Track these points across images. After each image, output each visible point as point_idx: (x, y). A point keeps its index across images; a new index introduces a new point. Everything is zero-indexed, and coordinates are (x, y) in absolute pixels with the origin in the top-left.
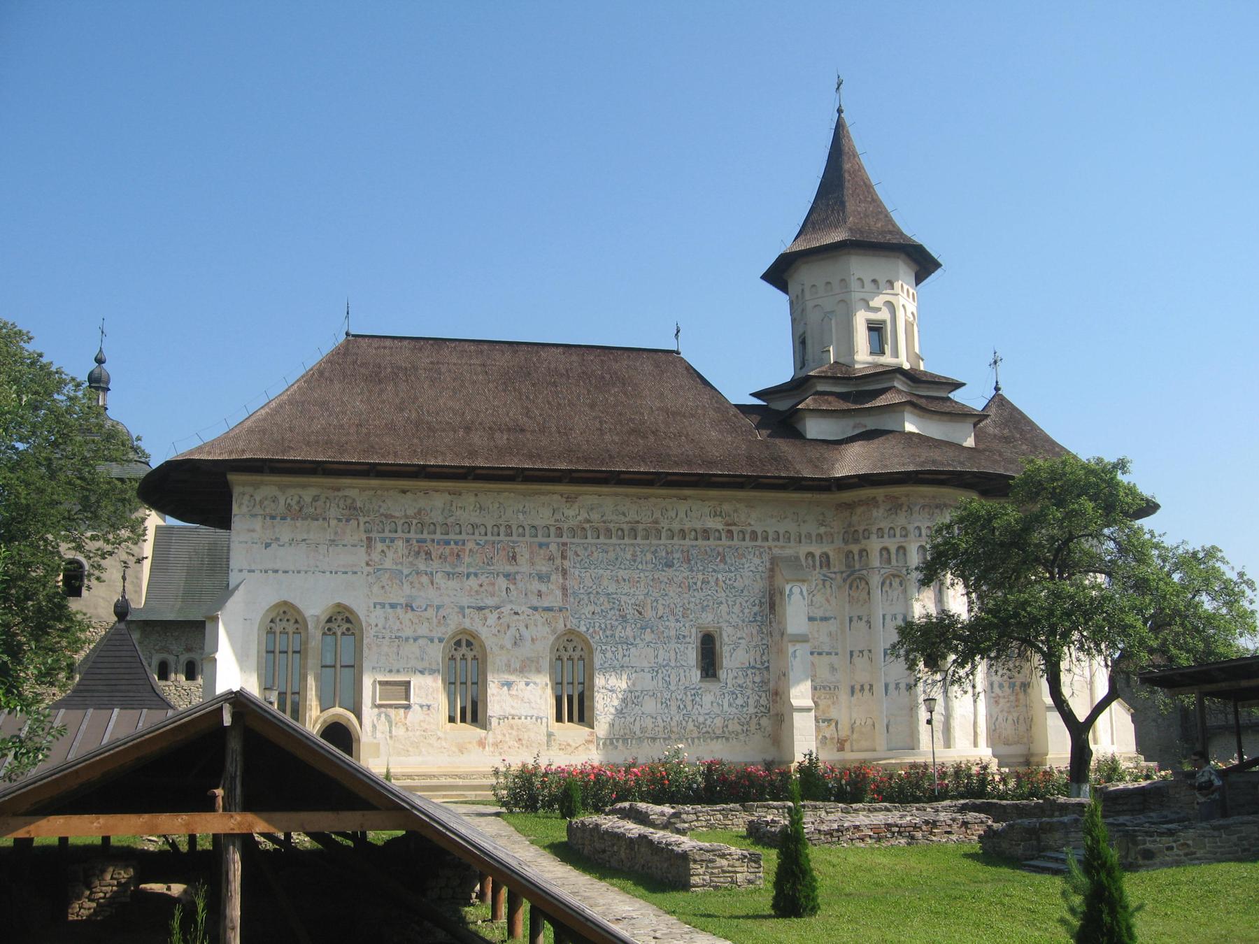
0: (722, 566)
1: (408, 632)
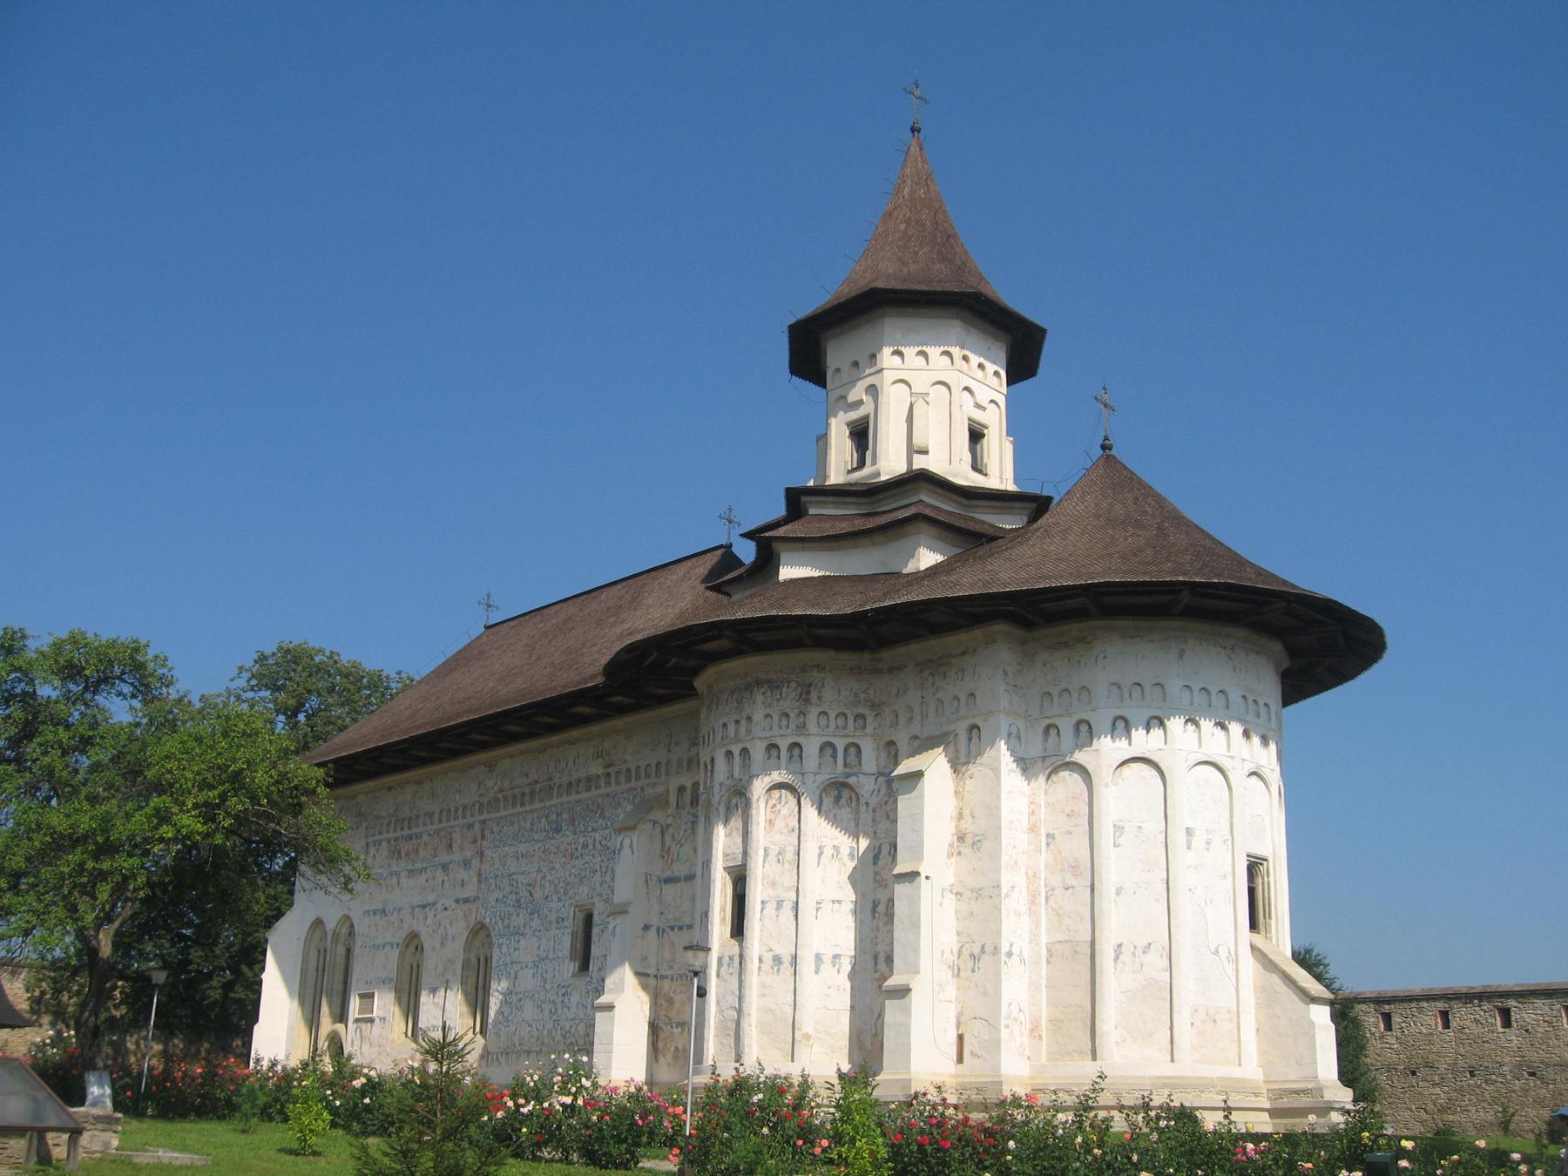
0: (601, 822)
1: (380, 941)
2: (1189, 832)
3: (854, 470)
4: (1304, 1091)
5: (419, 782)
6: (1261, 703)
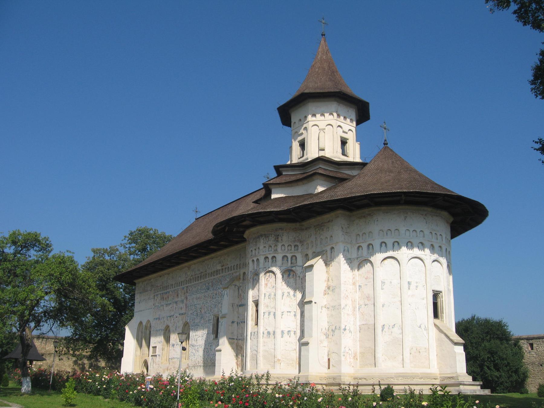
0: (221, 286)
1: (158, 329)
2: (409, 283)
3: (301, 158)
4: (452, 378)
5: (169, 274)
6: (438, 234)
